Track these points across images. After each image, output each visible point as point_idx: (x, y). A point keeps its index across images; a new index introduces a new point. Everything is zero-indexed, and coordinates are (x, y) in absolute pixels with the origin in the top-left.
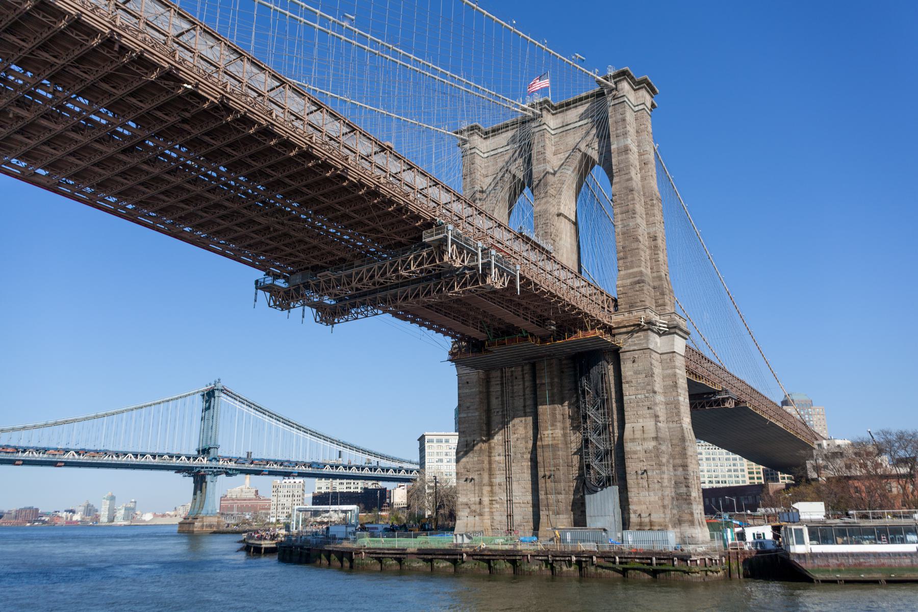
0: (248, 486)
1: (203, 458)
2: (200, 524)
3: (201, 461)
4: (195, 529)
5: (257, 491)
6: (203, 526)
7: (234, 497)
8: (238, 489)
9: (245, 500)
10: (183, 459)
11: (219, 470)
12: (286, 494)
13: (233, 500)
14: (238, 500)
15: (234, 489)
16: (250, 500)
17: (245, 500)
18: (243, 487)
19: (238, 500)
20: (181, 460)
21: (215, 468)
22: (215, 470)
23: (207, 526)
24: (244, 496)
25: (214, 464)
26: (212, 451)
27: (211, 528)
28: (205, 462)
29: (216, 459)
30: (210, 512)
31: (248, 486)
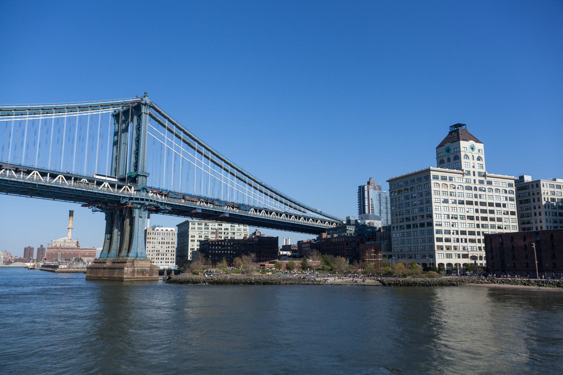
0: (70, 238)
1: (130, 188)
2: (130, 270)
3: (128, 190)
4: (125, 276)
5: (77, 242)
6: (133, 272)
7: (58, 246)
8: (61, 240)
9: (68, 249)
10: (106, 186)
11: (151, 203)
12: (161, 241)
13: (57, 248)
14: (62, 249)
15: (58, 240)
16: (72, 249)
17: (68, 249)
18: (66, 238)
19: (62, 249)
20: (104, 187)
21: (147, 200)
22: (147, 203)
23: (138, 272)
24: (67, 245)
25: (143, 195)
26: (140, 179)
27: (143, 274)
28: (132, 191)
29: (144, 189)
30: (139, 255)
31: (70, 238)
